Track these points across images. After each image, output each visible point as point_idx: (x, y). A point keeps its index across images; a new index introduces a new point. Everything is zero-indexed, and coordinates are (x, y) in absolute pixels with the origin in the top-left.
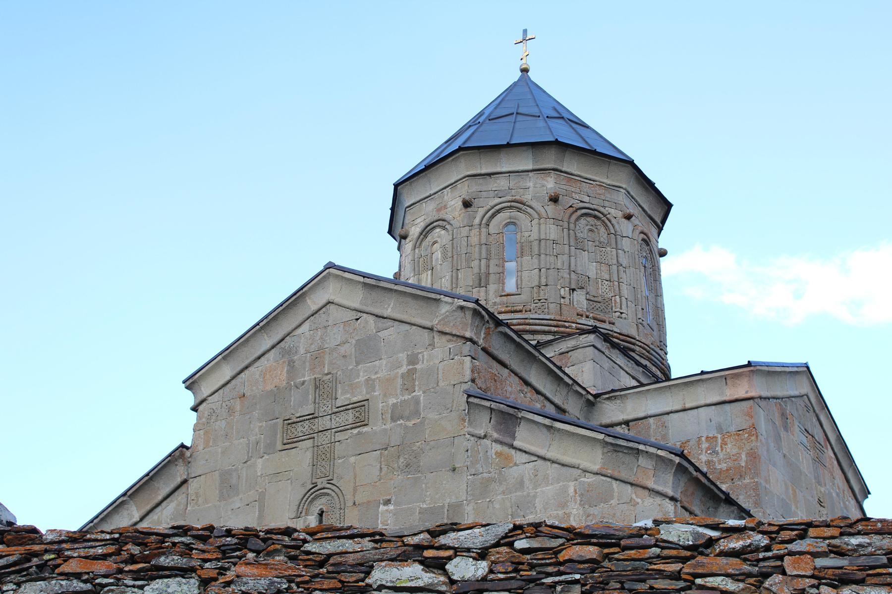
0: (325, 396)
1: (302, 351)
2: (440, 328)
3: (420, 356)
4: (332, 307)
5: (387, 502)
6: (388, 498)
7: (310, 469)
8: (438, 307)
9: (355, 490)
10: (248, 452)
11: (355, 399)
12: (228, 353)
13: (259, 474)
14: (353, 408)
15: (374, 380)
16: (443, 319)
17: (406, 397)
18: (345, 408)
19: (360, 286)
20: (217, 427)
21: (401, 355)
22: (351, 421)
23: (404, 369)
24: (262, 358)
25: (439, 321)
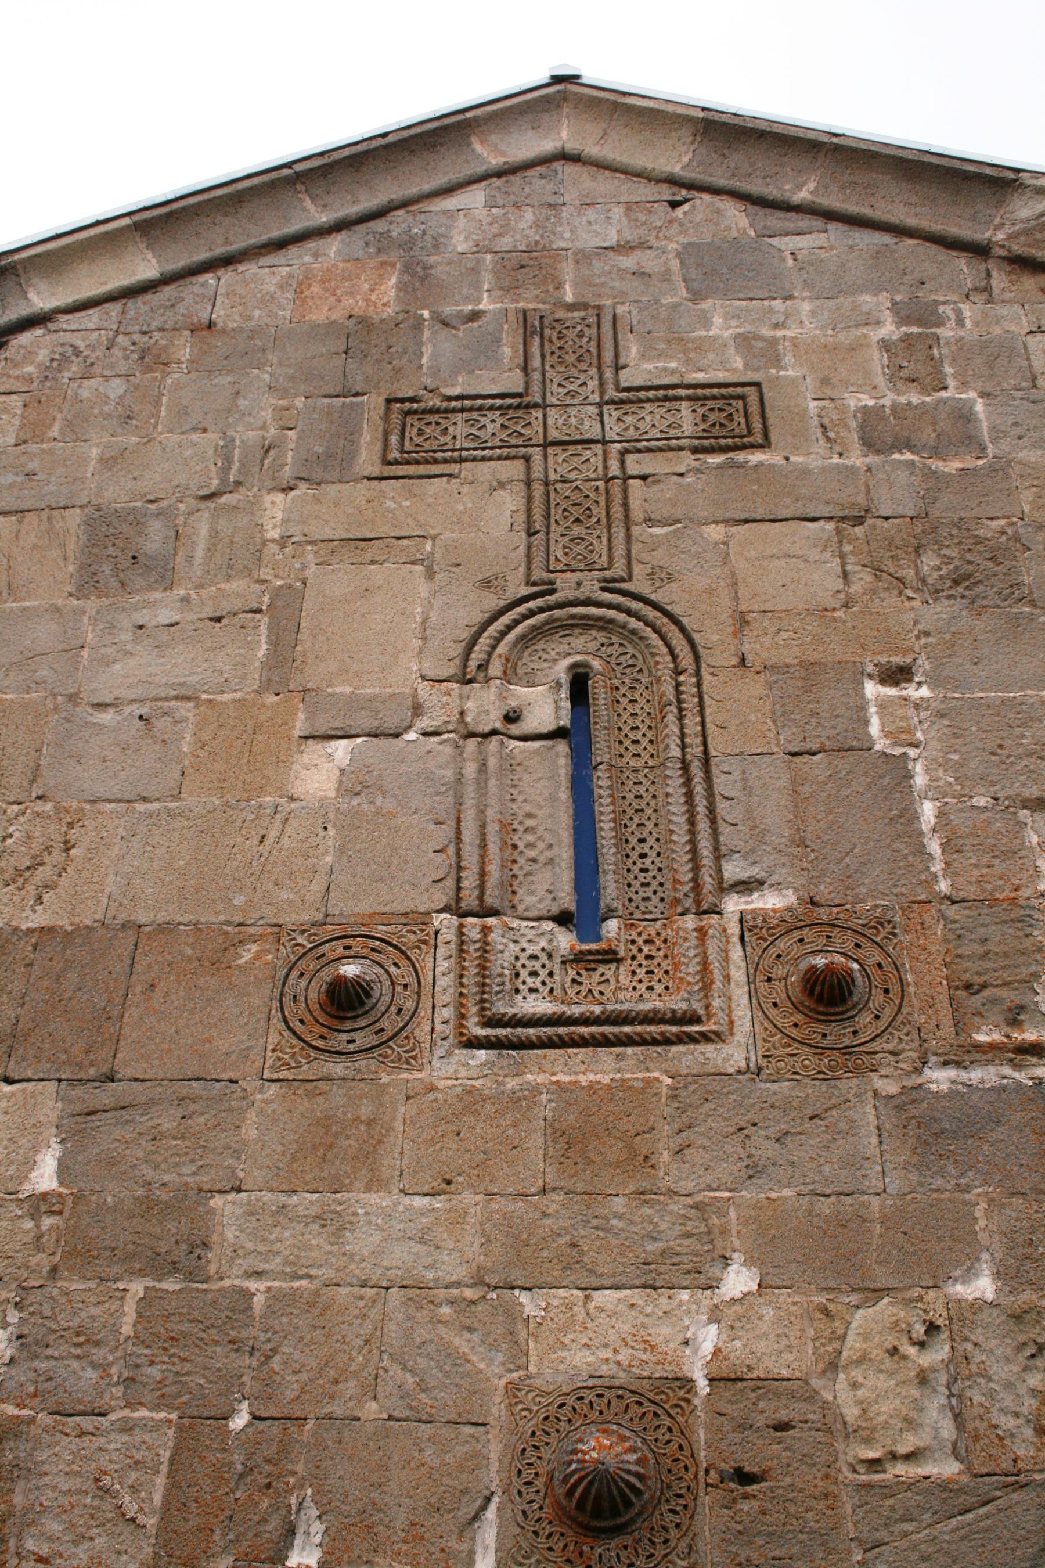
0: (571, 358)
1: (460, 244)
2: (1017, 249)
3: (946, 310)
4: (570, 170)
5: (897, 675)
6: (897, 660)
7: (520, 538)
8: (999, 204)
9: (742, 621)
10: (226, 469)
11: (700, 377)
12: (156, 222)
13: (274, 534)
14: (689, 398)
15: (773, 342)
16: (1026, 232)
17: (915, 399)
18: (665, 394)
19: (686, 134)
20: (85, 394)
21: (867, 298)
22: (688, 429)
23: (889, 329)
24: (293, 250)
25: (1009, 237)
